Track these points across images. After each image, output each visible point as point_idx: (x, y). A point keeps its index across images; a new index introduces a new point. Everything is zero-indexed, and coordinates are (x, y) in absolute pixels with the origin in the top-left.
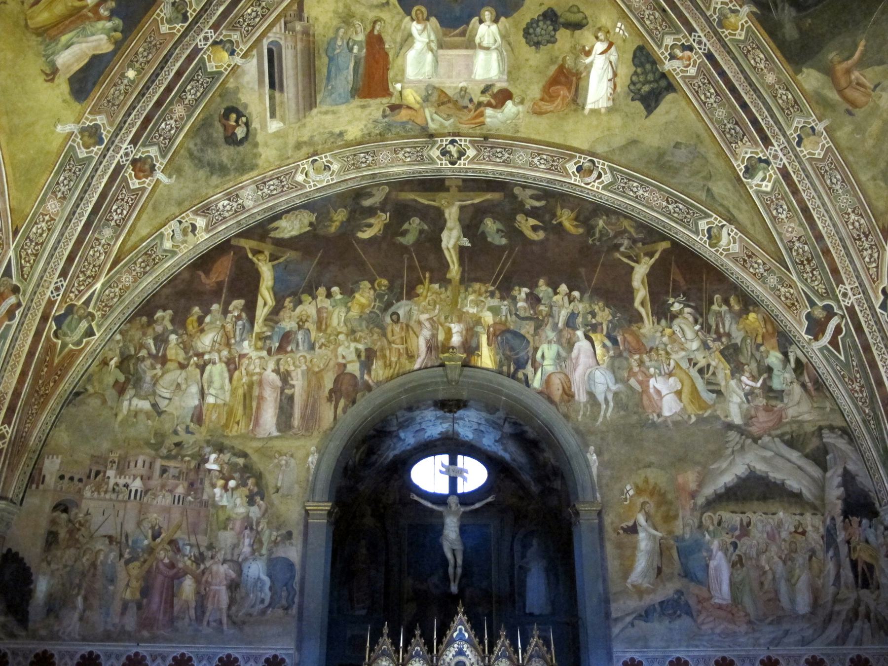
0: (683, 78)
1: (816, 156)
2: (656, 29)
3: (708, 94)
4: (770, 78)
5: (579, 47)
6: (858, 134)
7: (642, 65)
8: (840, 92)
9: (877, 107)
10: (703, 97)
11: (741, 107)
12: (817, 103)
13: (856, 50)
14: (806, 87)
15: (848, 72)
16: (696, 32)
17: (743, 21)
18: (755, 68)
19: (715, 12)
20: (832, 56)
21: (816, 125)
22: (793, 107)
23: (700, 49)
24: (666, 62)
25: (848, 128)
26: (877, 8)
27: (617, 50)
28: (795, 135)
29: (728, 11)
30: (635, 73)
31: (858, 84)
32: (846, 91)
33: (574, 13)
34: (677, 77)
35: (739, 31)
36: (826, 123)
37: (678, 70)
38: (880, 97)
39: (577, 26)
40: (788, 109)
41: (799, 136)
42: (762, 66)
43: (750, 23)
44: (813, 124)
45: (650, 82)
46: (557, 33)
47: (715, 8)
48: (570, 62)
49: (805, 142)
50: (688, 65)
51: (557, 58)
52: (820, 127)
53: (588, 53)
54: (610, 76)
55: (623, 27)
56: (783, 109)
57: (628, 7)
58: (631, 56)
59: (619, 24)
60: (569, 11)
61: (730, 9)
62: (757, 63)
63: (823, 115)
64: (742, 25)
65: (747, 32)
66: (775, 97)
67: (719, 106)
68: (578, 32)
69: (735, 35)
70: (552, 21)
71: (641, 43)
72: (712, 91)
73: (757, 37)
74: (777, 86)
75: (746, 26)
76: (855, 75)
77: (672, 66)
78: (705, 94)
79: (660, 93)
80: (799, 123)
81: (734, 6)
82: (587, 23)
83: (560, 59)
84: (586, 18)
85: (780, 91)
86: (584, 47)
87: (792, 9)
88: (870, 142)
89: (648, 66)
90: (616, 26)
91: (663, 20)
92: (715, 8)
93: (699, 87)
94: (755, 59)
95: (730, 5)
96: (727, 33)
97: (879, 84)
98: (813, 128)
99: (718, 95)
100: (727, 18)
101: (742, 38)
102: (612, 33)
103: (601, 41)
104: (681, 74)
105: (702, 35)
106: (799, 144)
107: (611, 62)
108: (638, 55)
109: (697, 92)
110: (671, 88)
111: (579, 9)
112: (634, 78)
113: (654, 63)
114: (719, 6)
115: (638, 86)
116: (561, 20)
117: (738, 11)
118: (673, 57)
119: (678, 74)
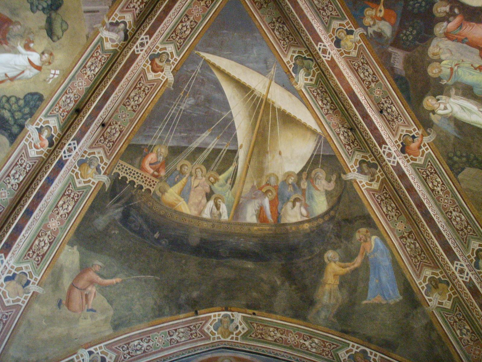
0: (25, 146)
1: (4, 300)
2: (60, 108)
3: (17, 176)
4: (54, 224)
5: (31, 37)
6: (45, 321)
7: (27, 104)
8: (73, 286)
9: (78, 320)
10: (13, 172)
11: (27, 210)
12: (53, 274)
13: (112, 278)
14: (62, 257)
15: (92, 282)
16: (78, 144)
17: (93, 180)
18: (57, 207)
19: (89, 154)
20: (98, 263)
21: (34, 283)
22: (38, 255)
23: (64, 152)
24: (34, 126)
25: (46, 310)
26: (148, 275)
27: (36, 76)
28: (13, 271)
29: (96, 165)
30: (18, 99)
31: (87, 296)
32: (76, 290)
33: (62, 27)
34: (24, 141)
35: (83, 180)
36: (39, 290)
37: (30, 140)
38: (85, 318)
39: (50, 33)
40: (34, 252)
41: (14, 275)
42: (62, 212)
43: (94, 187)
44: (32, 281)
45: (13, 117)
46: (41, 12)
47: (94, 153)
48: (16, 29)
49: (13, 283)
50: (36, 147)
51: (17, 15)
52: (33, 288)
53: (27, 47)
54: (10, 75)
55: (56, 76)
56: (31, 248)
57: (73, 77)
58: (33, 91)
59: (58, 72)
60: (63, 21)
61: (99, 165)
62: (62, 206)
63: (45, 285)
64: (89, 181)
65: (84, 188)
66: (39, 236)
67: (9, 190)
68: (44, 33)
69: (78, 178)
70: (51, 5)
71: (45, 97)
72: (21, 178)
73: (85, 196)
74: (49, 233)
75: (90, 184)
76: (92, 289)
77: (32, 132)
78: (16, 173)
79: (5, 130)
80: (27, 268)
81: (103, 168)
82: (54, 41)
83: (18, 19)
84: (59, 39)
85: (46, 238)
86: (33, 42)
87: (121, 214)
88: (45, 336)
89: (27, 110)
90: (56, 69)
91: (68, 112)
92: (94, 153)
93: (21, 165)
94: (64, 203)
95: (102, 165)
96: (77, 170)
97: (95, 311)
98: (28, 282)
99: (19, 185)
100: (90, 165)
101: (78, 185)
102: (49, 67)
103: (41, 58)
104: (27, 144)
105: (77, 150)
106: (7, 279)
107: (23, 72)
108: (35, 97)
109: (16, 164)
110: (13, 138)
111: (66, 30)
112: (13, 100)
113: (31, 114)
114: (97, 156)
115: (7, 106)
116: (53, 15)
117: (100, 173)
118: (40, 131)
119: (27, 140)
